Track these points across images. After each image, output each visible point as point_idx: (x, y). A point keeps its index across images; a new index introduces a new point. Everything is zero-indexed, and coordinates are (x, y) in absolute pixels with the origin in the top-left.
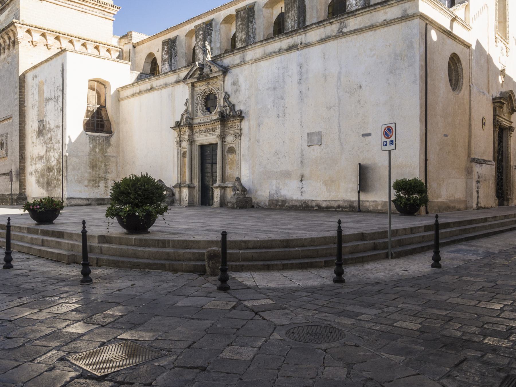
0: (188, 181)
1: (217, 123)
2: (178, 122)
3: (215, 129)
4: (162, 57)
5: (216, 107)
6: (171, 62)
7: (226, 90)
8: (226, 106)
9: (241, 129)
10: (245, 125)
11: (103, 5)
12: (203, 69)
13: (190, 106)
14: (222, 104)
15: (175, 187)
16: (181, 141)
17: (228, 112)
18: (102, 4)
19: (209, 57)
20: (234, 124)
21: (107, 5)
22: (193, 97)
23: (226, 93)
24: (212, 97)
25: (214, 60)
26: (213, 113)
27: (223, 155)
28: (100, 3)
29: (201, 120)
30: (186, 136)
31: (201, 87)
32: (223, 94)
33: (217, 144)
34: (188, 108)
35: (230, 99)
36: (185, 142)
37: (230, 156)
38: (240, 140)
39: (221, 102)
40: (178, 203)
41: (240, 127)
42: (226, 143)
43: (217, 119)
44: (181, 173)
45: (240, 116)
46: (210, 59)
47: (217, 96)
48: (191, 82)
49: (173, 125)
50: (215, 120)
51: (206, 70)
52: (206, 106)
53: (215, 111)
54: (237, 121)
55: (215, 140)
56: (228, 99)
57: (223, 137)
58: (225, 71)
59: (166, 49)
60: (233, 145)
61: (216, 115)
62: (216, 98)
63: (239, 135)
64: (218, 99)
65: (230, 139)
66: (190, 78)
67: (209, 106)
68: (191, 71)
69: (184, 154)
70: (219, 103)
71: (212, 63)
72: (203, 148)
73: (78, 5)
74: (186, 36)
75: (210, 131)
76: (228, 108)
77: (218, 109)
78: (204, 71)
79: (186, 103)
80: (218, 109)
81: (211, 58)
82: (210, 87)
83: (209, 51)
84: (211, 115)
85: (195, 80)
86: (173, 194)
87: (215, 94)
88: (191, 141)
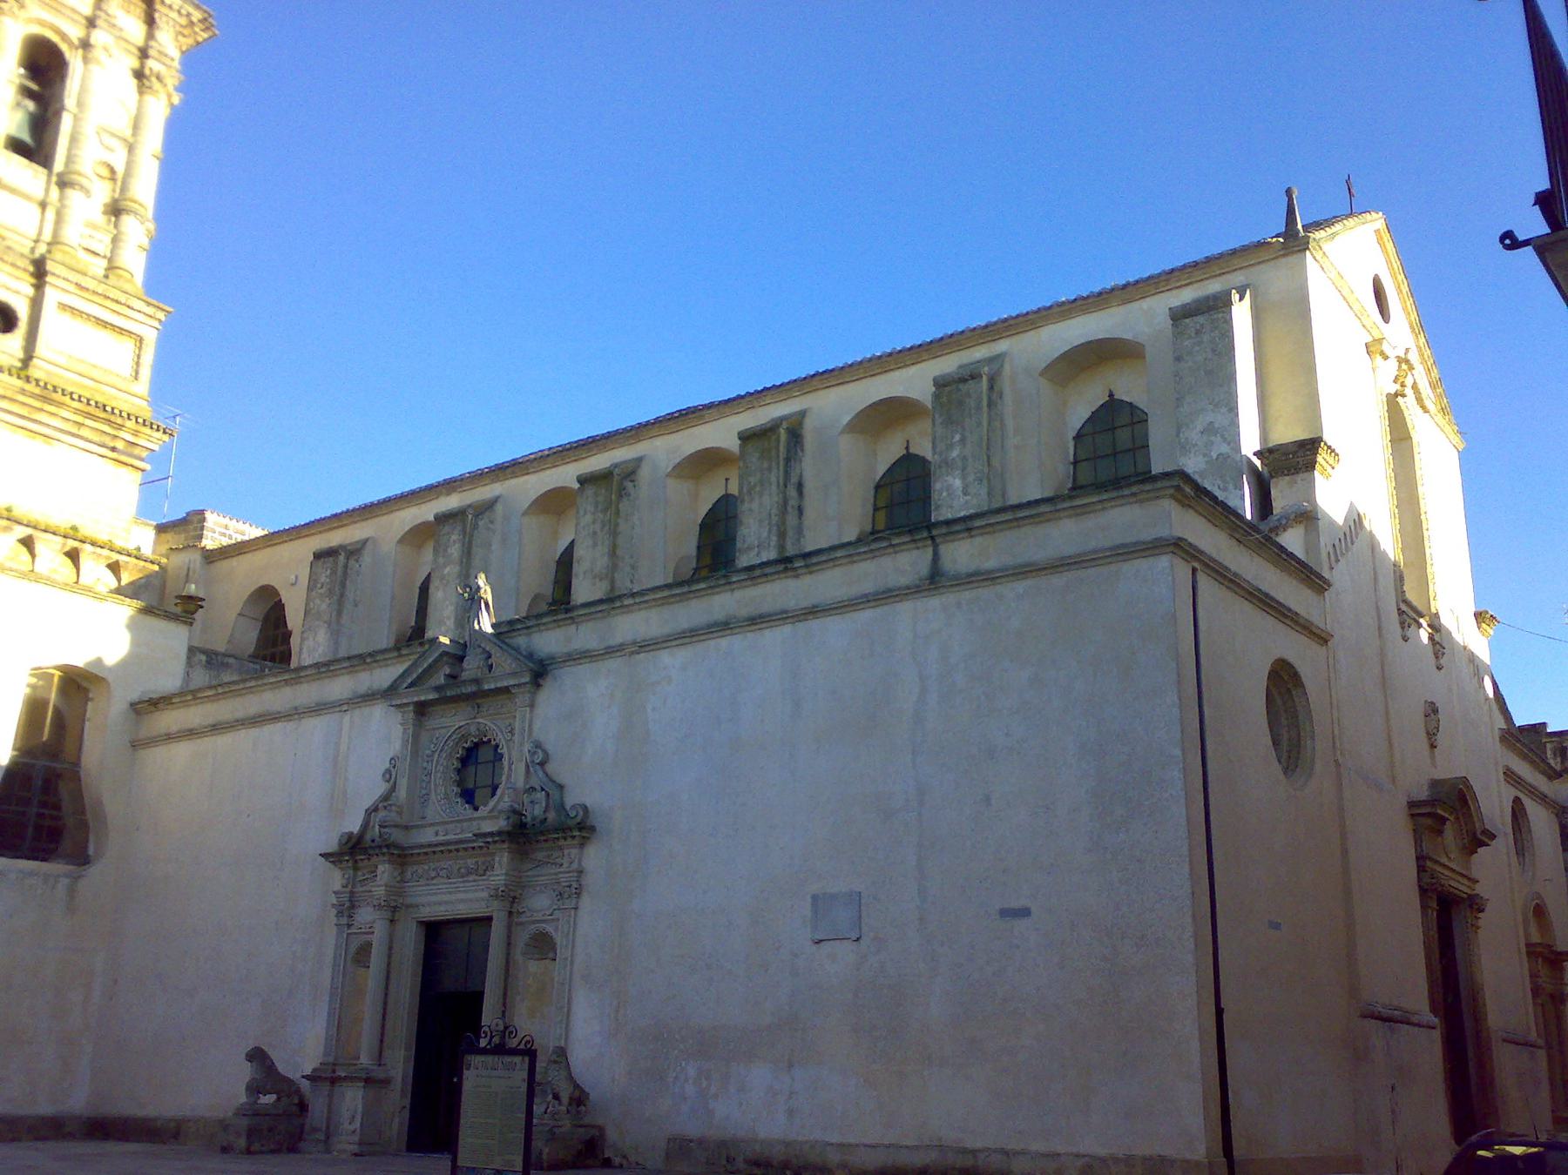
0: (365, 1060)
1: (498, 846)
2: (350, 835)
3: (489, 867)
4: (307, 604)
5: (495, 788)
6: (338, 622)
7: (538, 733)
8: (533, 789)
9: (580, 872)
10: (593, 858)
11: (112, 418)
12: (461, 659)
13: (403, 784)
14: (520, 783)
15: (313, 1078)
16: (353, 907)
17: (538, 811)
18: (113, 413)
19: (486, 623)
20: (556, 854)
21: (144, 425)
22: (415, 753)
23: (538, 745)
24: (485, 754)
25: (504, 629)
26: (483, 811)
27: (508, 962)
28: (105, 410)
29: (437, 834)
30: (379, 891)
31: (451, 723)
32: (527, 747)
33: (488, 920)
34: (393, 788)
35: (550, 768)
36: (370, 909)
37: (534, 967)
38: (576, 909)
39: (514, 773)
40: (318, 1141)
41: (580, 864)
42: (523, 919)
43: (499, 833)
44: (340, 1027)
45: (580, 828)
46: (488, 629)
47: (504, 750)
48: (416, 699)
49: (332, 846)
50: (491, 834)
51: (472, 666)
52: (459, 783)
53: (492, 803)
54: (569, 841)
55: (483, 904)
56: (542, 764)
57: (512, 898)
58: (540, 671)
59: (323, 579)
60: (549, 929)
61: (497, 818)
62: (499, 757)
63: (572, 891)
64: (505, 762)
65: (539, 903)
66: (411, 685)
67: (471, 786)
68: (414, 665)
69: (362, 955)
70: (509, 776)
71: (495, 640)
72: (434, 931)
73: (24, 411)
74: (401, 541)
75: (469, 873)
76: (541, 796)
77: (504, 799)
78: (465, 665)
79: (388, 771)
80: (504, 799)
81: (493, 626)
82: (481, 720)
83: (487, 604)
84: (476, 814)
85: (432, 696)
86: (303, 1107)
87: (497, 746)
88: (394, 910)
